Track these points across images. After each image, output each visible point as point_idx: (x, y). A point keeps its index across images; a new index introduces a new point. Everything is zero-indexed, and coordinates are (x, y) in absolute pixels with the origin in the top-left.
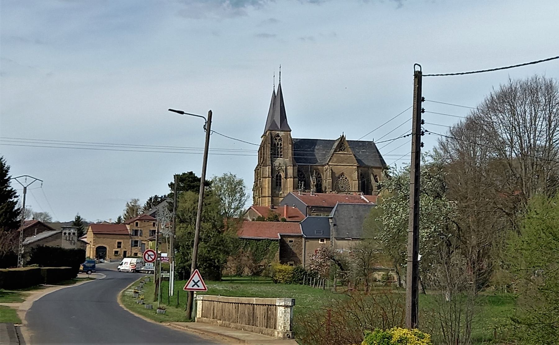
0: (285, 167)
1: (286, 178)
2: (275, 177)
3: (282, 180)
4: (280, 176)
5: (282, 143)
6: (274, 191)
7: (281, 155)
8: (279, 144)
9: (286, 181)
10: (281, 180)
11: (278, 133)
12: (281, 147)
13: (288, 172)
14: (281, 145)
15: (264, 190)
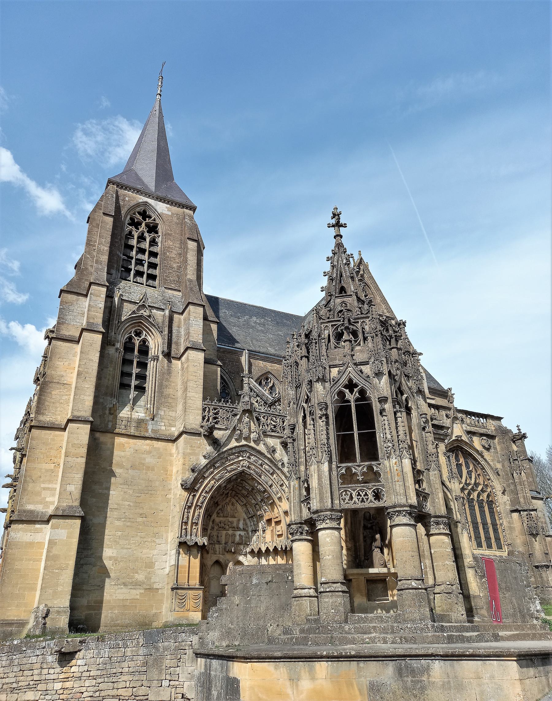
0: (167, 312)
1: (168, 355)
2: (118, 345)
3: (151, 365)
4: (144, 350)
5: (159, 240)
6: (110, 402)
7: (152, 277)
8: (148, 240)
9: (169, 372)
10: (143, 365)
11: (146, 204)
12: (154, 249)
13: (179, 337)
14: (153, 242)
15: (55, 393)
